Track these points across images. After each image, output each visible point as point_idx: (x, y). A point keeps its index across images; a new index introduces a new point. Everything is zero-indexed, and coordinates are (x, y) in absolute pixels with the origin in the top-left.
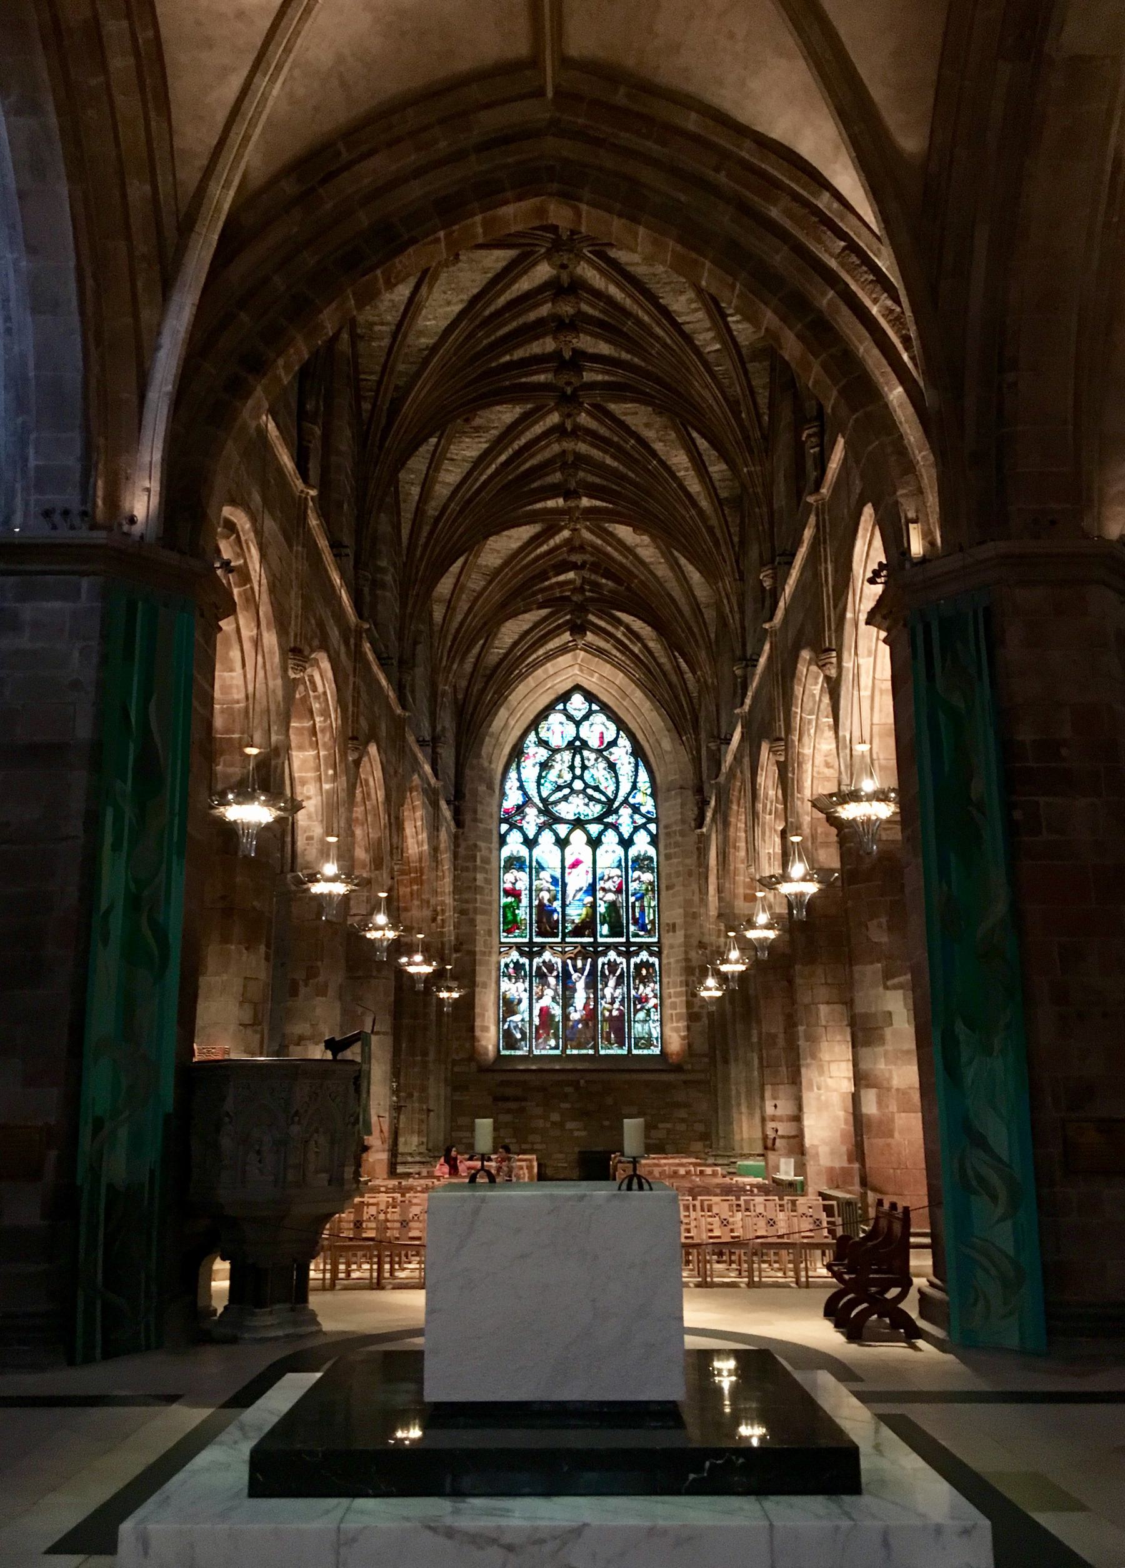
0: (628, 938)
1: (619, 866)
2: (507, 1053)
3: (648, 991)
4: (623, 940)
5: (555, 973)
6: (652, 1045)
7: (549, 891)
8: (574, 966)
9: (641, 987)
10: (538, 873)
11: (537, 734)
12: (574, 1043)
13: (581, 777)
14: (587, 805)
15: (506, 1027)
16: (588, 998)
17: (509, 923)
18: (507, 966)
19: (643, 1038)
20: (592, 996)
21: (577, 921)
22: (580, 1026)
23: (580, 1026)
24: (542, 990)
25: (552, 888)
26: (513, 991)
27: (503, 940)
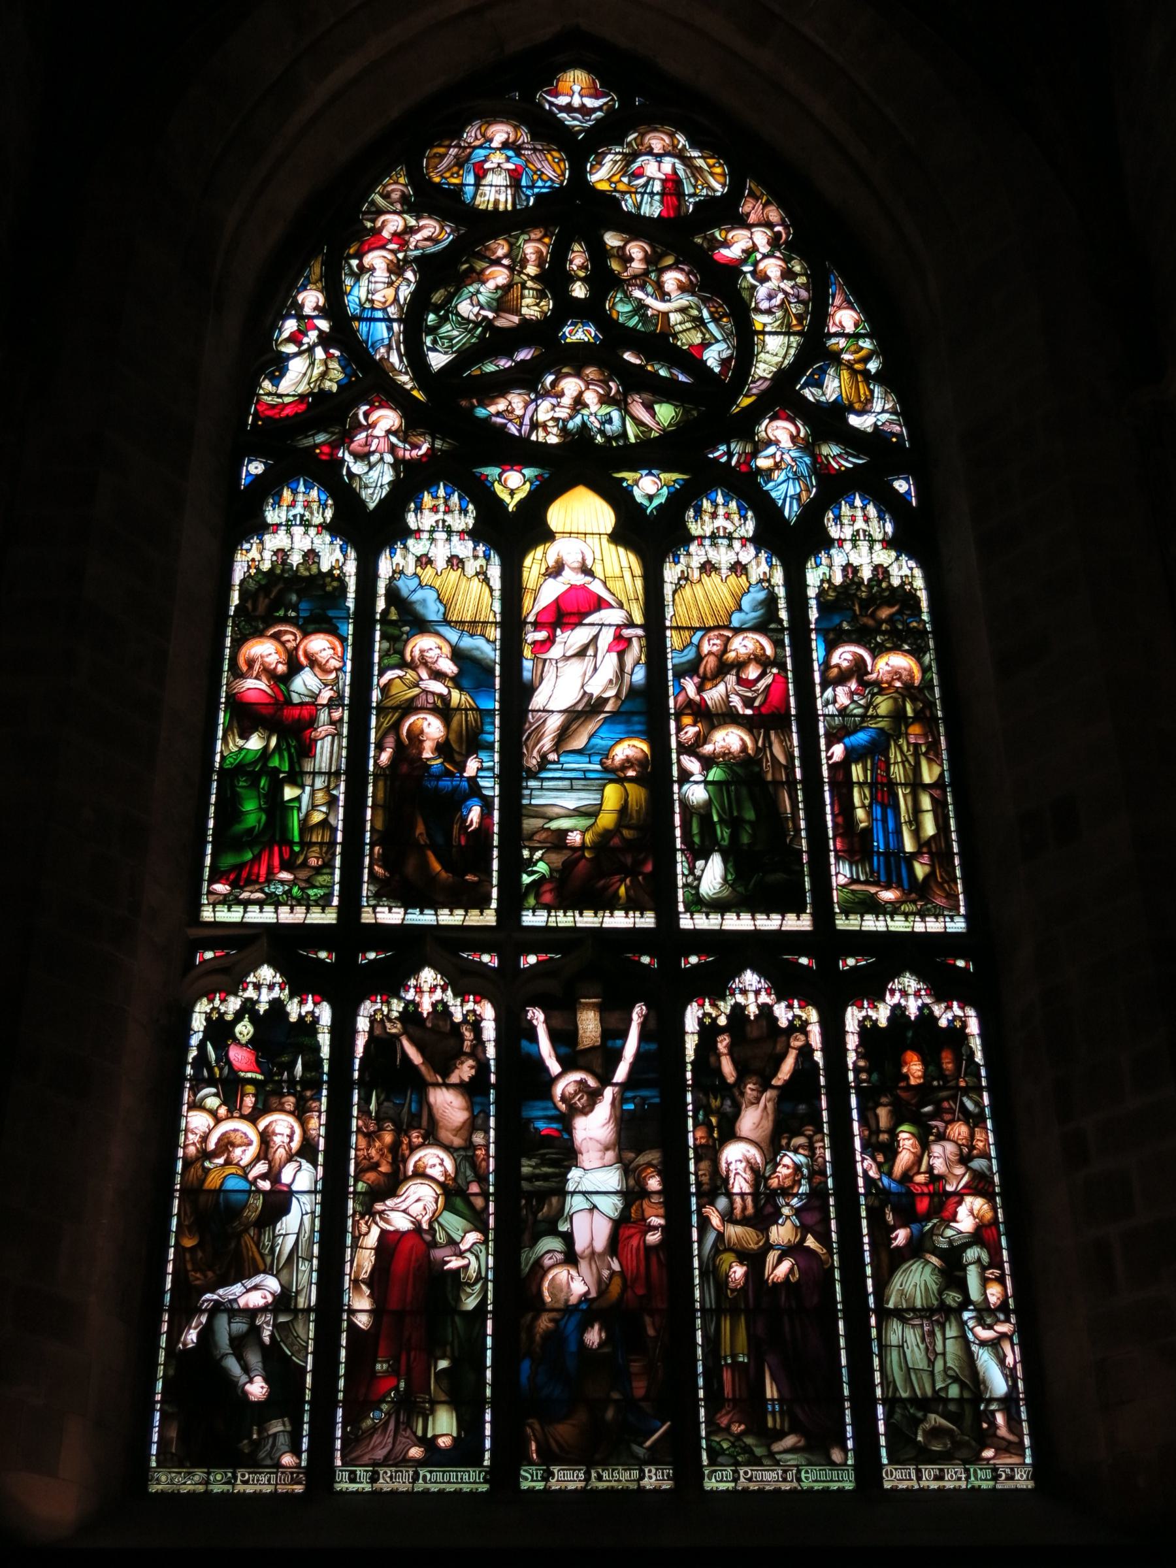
0: (823, 916)
1: (765, 624)
2: (189, 1483)
3: (940, 1156)
4: (801, 923)
5: (465, 1071)
6: (987, 1437)
7: (444, 710)
8: (564, 1038)
9: (906, 1139)
10: (396, 643)
11: (418, 179)
12: (564, 1431)
13: (591, 311)
14: (621, 403)
15: (192, 1336)
16: (632, 1195)
17: (250, 839)
18: (220, 1030)
19: (936, 1401)
20: (654, 1184)
21: (575, 838)
22: (593, 1337)
23: (593, 1337)
24: (398, 1156)
25: (456, 697)
26: (245, 1155)
27: (207, 915)
